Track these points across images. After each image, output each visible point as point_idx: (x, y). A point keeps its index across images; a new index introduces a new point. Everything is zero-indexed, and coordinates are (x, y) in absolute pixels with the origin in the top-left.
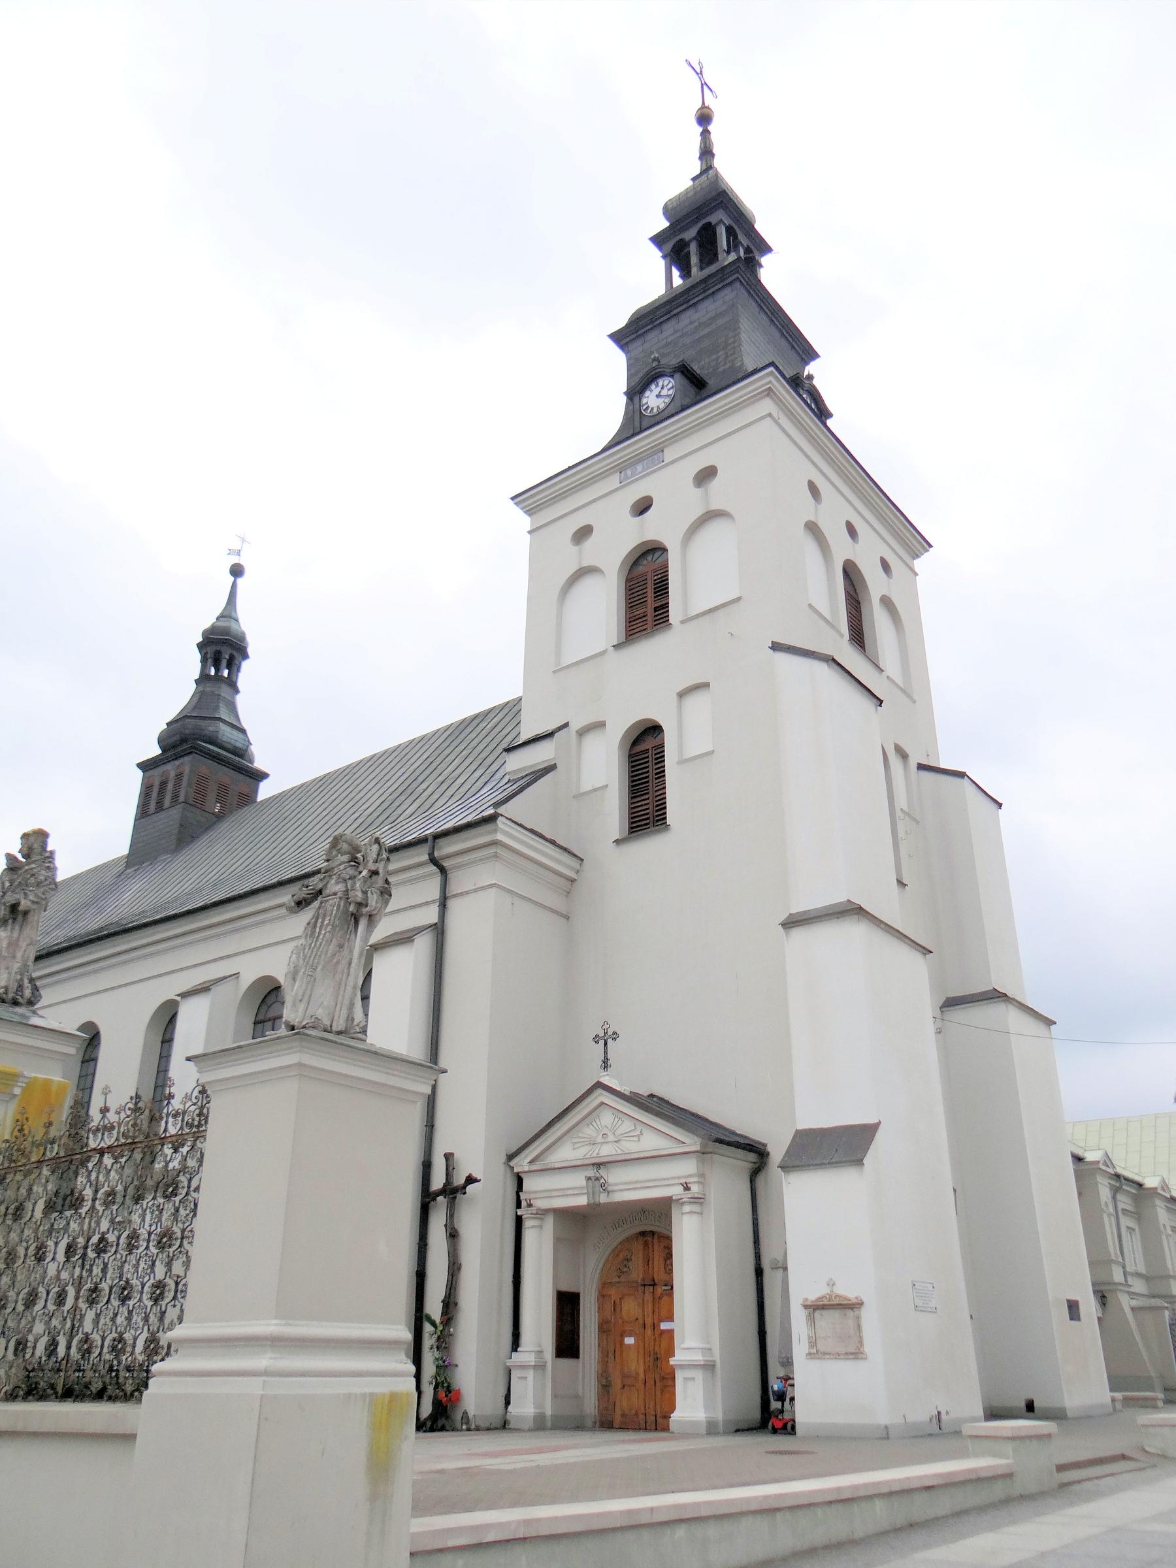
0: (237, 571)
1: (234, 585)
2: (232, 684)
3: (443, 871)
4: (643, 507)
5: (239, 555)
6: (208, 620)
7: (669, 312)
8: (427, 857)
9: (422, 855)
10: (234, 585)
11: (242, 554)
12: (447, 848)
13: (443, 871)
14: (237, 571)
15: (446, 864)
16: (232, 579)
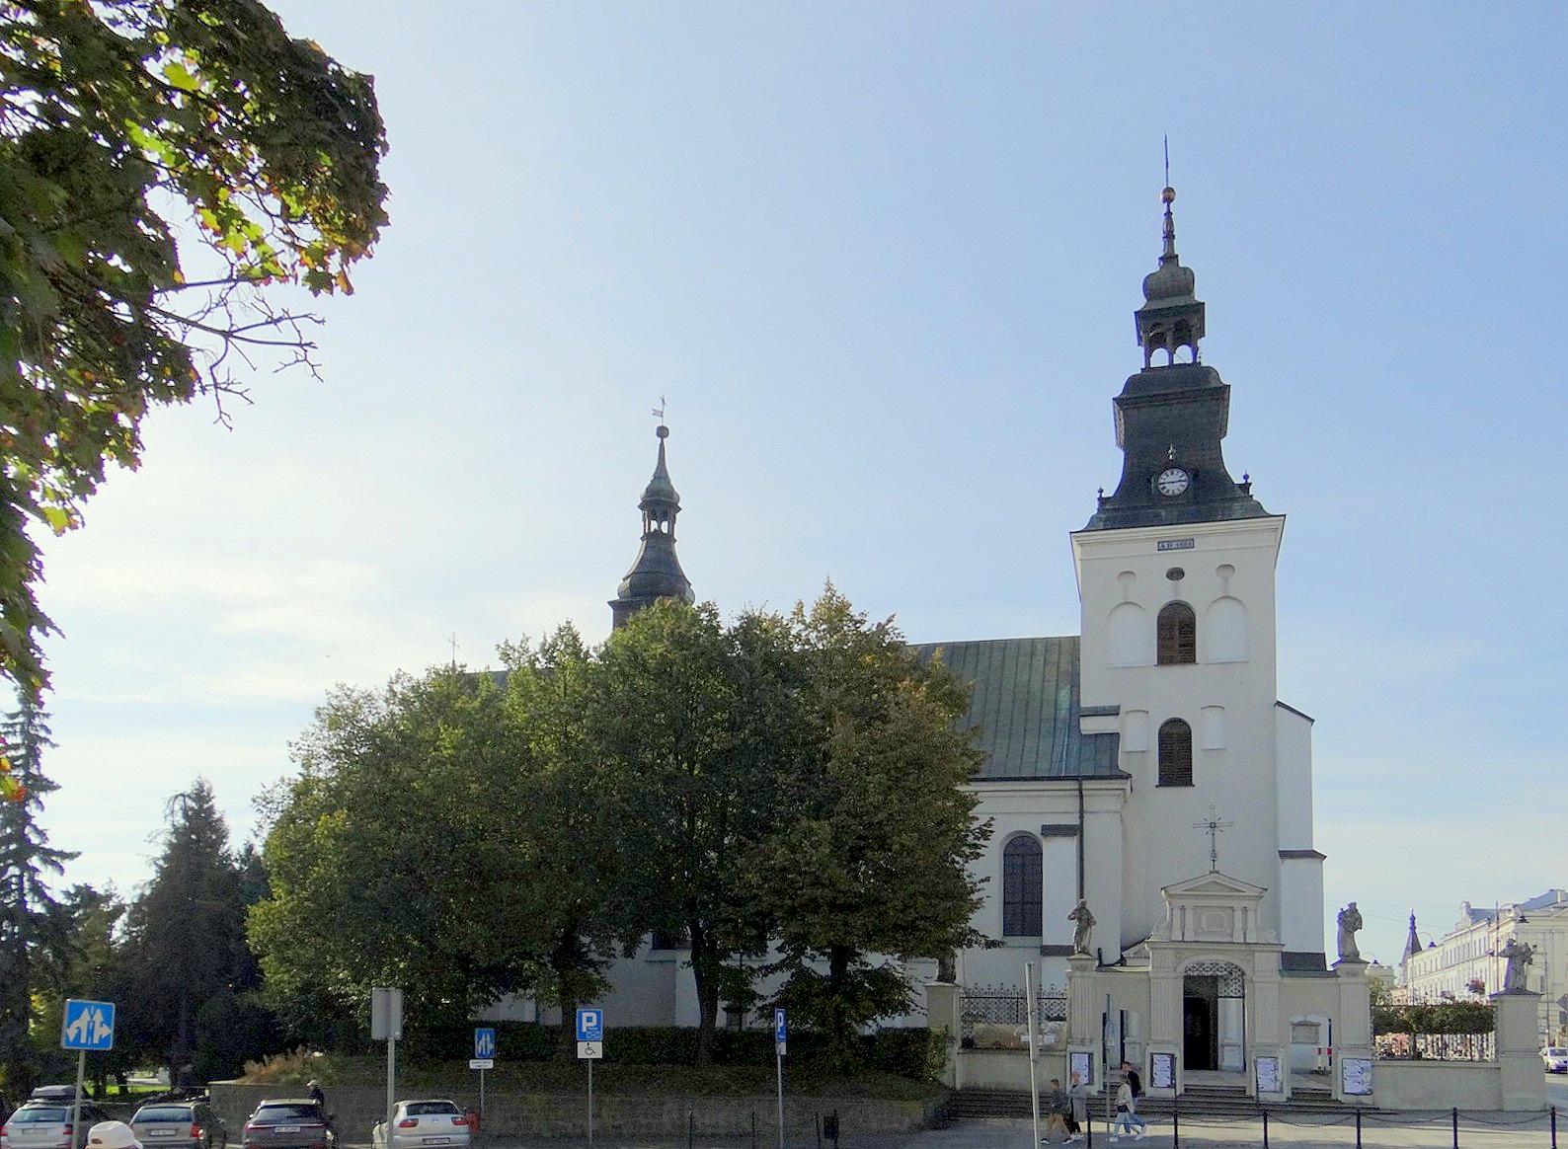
0: (662, 432)
1: (662, 444)
2: (669, 538)
3: (1081, 797)
4: (1176, 574)
5: (662, 416)
6: (646, 480)
7: (1165, 400)
8: (1077, 787)
9: (1073, 785)
10: (662, 444)
11: (664, 415)
12: (1086, 785)
13: (1081, 797)
14: (662, 432)
15: (1084, 793)
16: (659, 439)
